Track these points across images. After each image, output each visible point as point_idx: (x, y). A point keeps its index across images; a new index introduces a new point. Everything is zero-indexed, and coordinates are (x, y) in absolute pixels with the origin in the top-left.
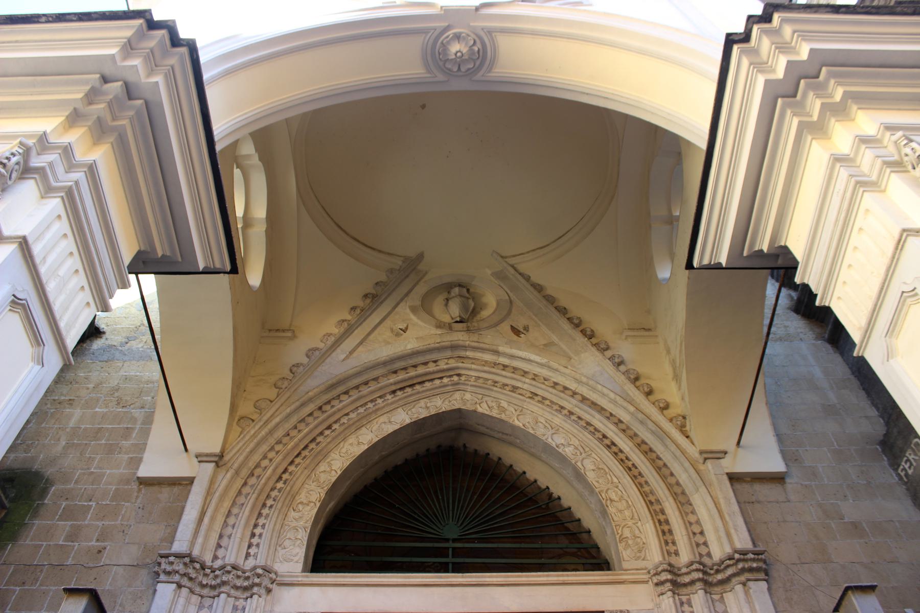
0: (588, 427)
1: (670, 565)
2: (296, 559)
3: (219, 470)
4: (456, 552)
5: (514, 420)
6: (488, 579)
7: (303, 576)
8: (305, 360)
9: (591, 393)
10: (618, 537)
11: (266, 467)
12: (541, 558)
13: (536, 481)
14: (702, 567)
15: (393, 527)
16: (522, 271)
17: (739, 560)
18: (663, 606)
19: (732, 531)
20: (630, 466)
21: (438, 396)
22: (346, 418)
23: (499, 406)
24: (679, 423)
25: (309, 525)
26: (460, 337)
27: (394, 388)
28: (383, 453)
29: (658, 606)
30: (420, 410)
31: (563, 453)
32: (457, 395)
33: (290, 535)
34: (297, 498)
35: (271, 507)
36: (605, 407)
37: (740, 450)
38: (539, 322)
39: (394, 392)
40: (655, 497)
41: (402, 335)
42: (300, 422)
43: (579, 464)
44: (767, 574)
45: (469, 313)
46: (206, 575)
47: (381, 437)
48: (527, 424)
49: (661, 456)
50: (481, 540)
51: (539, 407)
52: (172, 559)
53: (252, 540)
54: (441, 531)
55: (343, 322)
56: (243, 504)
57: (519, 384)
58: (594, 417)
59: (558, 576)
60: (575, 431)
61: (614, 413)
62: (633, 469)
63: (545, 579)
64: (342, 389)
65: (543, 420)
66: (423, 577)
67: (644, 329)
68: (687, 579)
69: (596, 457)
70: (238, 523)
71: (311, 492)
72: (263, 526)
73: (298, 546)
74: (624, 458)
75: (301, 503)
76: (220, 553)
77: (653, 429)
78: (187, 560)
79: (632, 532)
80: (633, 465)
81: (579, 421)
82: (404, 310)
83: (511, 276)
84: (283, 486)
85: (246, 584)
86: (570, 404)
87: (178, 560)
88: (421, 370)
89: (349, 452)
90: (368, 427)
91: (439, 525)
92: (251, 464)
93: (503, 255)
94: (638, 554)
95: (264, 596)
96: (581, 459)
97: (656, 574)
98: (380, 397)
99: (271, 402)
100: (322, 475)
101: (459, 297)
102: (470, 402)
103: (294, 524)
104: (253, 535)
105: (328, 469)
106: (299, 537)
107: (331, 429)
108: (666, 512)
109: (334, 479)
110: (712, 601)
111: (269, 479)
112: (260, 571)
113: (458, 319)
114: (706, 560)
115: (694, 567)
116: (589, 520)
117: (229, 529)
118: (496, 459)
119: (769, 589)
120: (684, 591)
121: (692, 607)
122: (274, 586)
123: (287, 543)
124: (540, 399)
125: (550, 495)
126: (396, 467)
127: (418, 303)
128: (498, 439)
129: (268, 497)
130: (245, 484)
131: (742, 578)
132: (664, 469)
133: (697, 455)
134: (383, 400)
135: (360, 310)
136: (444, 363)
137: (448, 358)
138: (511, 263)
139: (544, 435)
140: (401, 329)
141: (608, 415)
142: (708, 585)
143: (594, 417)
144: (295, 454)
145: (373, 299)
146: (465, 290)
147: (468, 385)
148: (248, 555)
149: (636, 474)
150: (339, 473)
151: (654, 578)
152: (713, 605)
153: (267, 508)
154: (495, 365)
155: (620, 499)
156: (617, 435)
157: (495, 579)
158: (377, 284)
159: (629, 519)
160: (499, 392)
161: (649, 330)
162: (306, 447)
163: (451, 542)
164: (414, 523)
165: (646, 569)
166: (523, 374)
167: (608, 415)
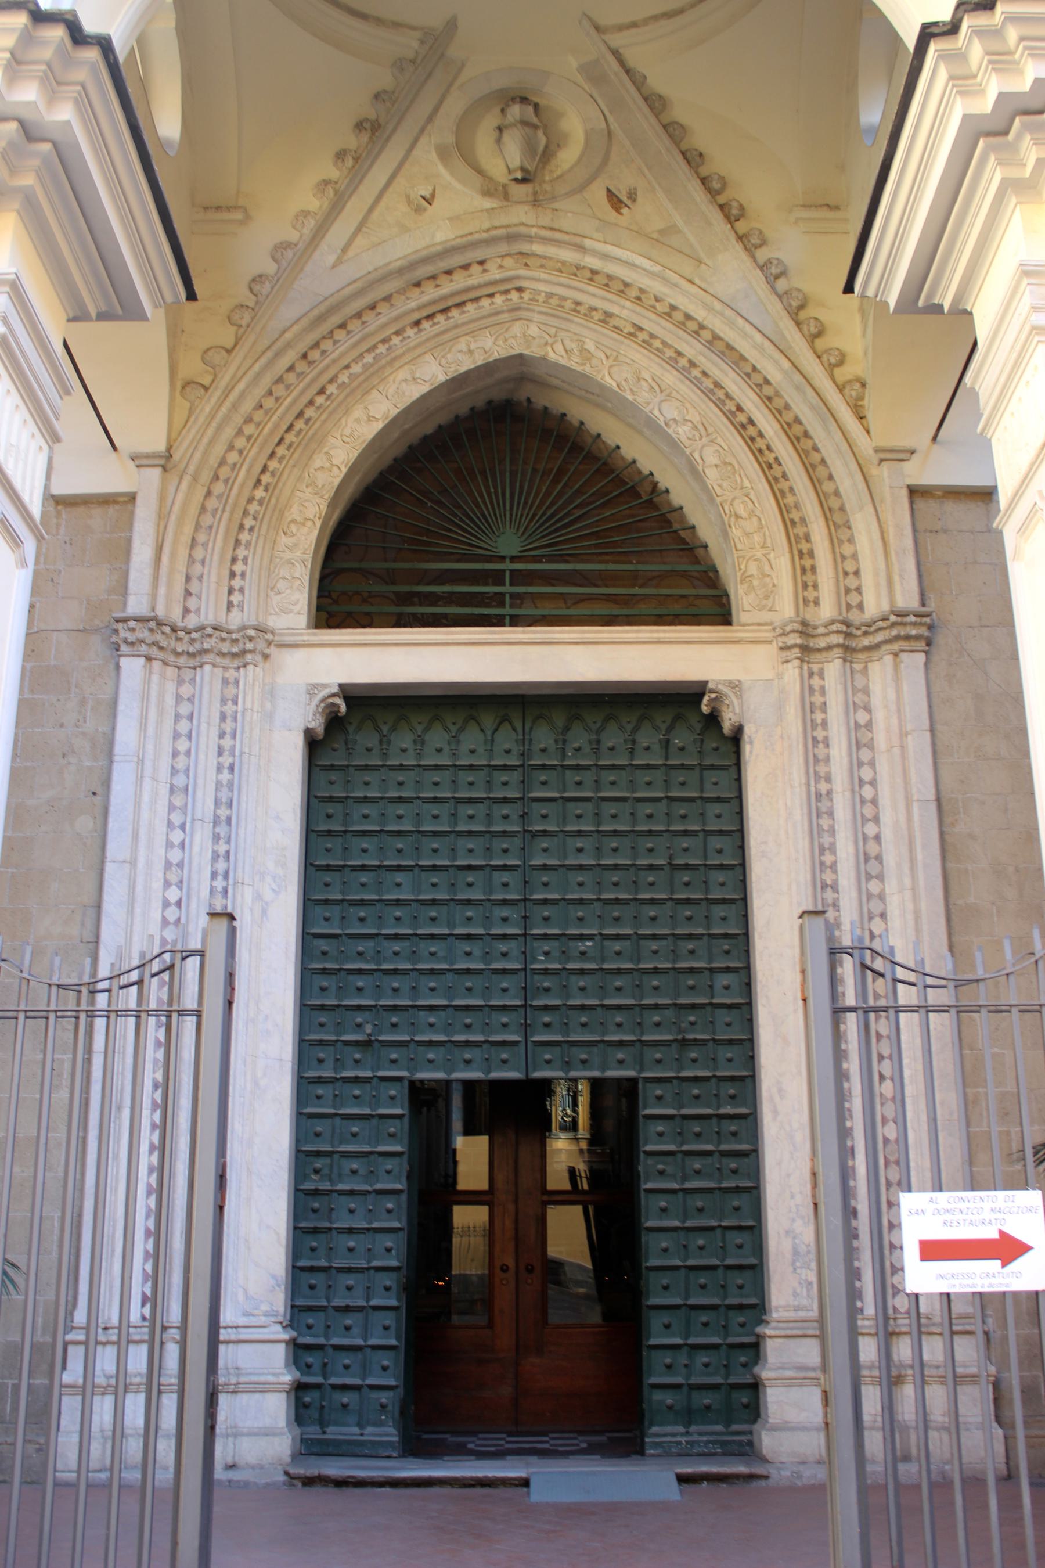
0: (716, 390)
1: (804, 623)
2: (296, 609)
4: (518, 578)
7: (309, 634)
8: (271, 268)
10: (739, 574)
11: (235, 465)
12: (634, 586)
13: (634, 462)
14: (844, 628)
15: (425, 538)
16: (631, 63)
17: (894, 625)
18: (786, 678)
19: (896, 578)
20: (772, 461)
21: (487, 331)
22: (346, 372)
23: (583, 350)
24: (854, 393)
25: (309, 557)
26: (520, 215)
27: (416, 316)
28: (406, 426)
29: (780, 676)
30: (460, 356)
31: (674, 436)
32: (517, 328)
33: (284, 572)
34: (286, 514)
35: (252, 529)
37: (935, 447)
39: (417, 323)
40: (800, 514)
41: (425, 210)
43: (696, 455)
44: (928, 644)
45: (537, 158)
47: (402, 406)
48: (623, 383)
49: (819, 446)
50: (551, 559)
52: (132, 624)
53: (233, 583)
55: (326, 185)
56: (211, 527)
57: (614, 309)
58: (727, 375)
59: (651, 631)
61: (758, 367)
62: (775, 466)
64: (335, 320)
65: (648, 377)
66: (470, 633)
67: (828, 205)
68: (822, 643)
69: (723, 444)
72: (245, 560)
74: (764, 448)
75: (294, 521)
76: (192, 603)
78: (153, 624)
79: (760, 568)
80: (776, 459)
81: (704, 379)
82: (426, 153)
84: (264, 494)
85: (235, 650)
86: (691, 348)
87: (140, 625)
88: (460, 281)
89: (356, 433)
91: (487, 541)
92: (213, 461)
93: (602, 22)
94: (764, 602)
95: (261, 665)
97: (783, 634)
98: (397, 333)
99: (229, 352)
101: (519, 126)
103: (288, 555)
104: (233, 575)
105: (327, 465)
106: (297, 575)
108: (813, 539)
109: (337, 482)
110: (852, 672)
111: (242, 486)
112: (251, 632)
114: (855, 617)
115: (834, 627)
116: (706, 532)
117: (197, 569)
119: (926, 664)
120: (818, 656)
121: (823, 679)
122: (272, 651)
123: (281, 585)
124: (647, 338)
125: (655, 485)
126: (425, 439)
127: (451, 139)
129: (245, 513)
130: (209, 493)
131: (896, 647)
132: (820, 469)
133: (871, 452)
134: (400, 338)
137: (503, 256)
138: (614, 44)
139: (648, 404)
140: (424, 198)
141: (749, 370)
142: (848, 651)
143: (727, 375)
144: (276, 440)
145: (373, 134)
146: (531, 109)
147: (533, 311)
148: (230, 605)
149: (779, 475)
150: (344, 470)
151: (780, 639)
152: (852, 678)
154: (578, 269)
155: (749, 515)
157: (566, 636)
158: (377, 96)
161: (837, 208)
162: (290, 428)
163: (508, 560)
165: (771, 624)
166: (622, 287)
167: (749, 370)
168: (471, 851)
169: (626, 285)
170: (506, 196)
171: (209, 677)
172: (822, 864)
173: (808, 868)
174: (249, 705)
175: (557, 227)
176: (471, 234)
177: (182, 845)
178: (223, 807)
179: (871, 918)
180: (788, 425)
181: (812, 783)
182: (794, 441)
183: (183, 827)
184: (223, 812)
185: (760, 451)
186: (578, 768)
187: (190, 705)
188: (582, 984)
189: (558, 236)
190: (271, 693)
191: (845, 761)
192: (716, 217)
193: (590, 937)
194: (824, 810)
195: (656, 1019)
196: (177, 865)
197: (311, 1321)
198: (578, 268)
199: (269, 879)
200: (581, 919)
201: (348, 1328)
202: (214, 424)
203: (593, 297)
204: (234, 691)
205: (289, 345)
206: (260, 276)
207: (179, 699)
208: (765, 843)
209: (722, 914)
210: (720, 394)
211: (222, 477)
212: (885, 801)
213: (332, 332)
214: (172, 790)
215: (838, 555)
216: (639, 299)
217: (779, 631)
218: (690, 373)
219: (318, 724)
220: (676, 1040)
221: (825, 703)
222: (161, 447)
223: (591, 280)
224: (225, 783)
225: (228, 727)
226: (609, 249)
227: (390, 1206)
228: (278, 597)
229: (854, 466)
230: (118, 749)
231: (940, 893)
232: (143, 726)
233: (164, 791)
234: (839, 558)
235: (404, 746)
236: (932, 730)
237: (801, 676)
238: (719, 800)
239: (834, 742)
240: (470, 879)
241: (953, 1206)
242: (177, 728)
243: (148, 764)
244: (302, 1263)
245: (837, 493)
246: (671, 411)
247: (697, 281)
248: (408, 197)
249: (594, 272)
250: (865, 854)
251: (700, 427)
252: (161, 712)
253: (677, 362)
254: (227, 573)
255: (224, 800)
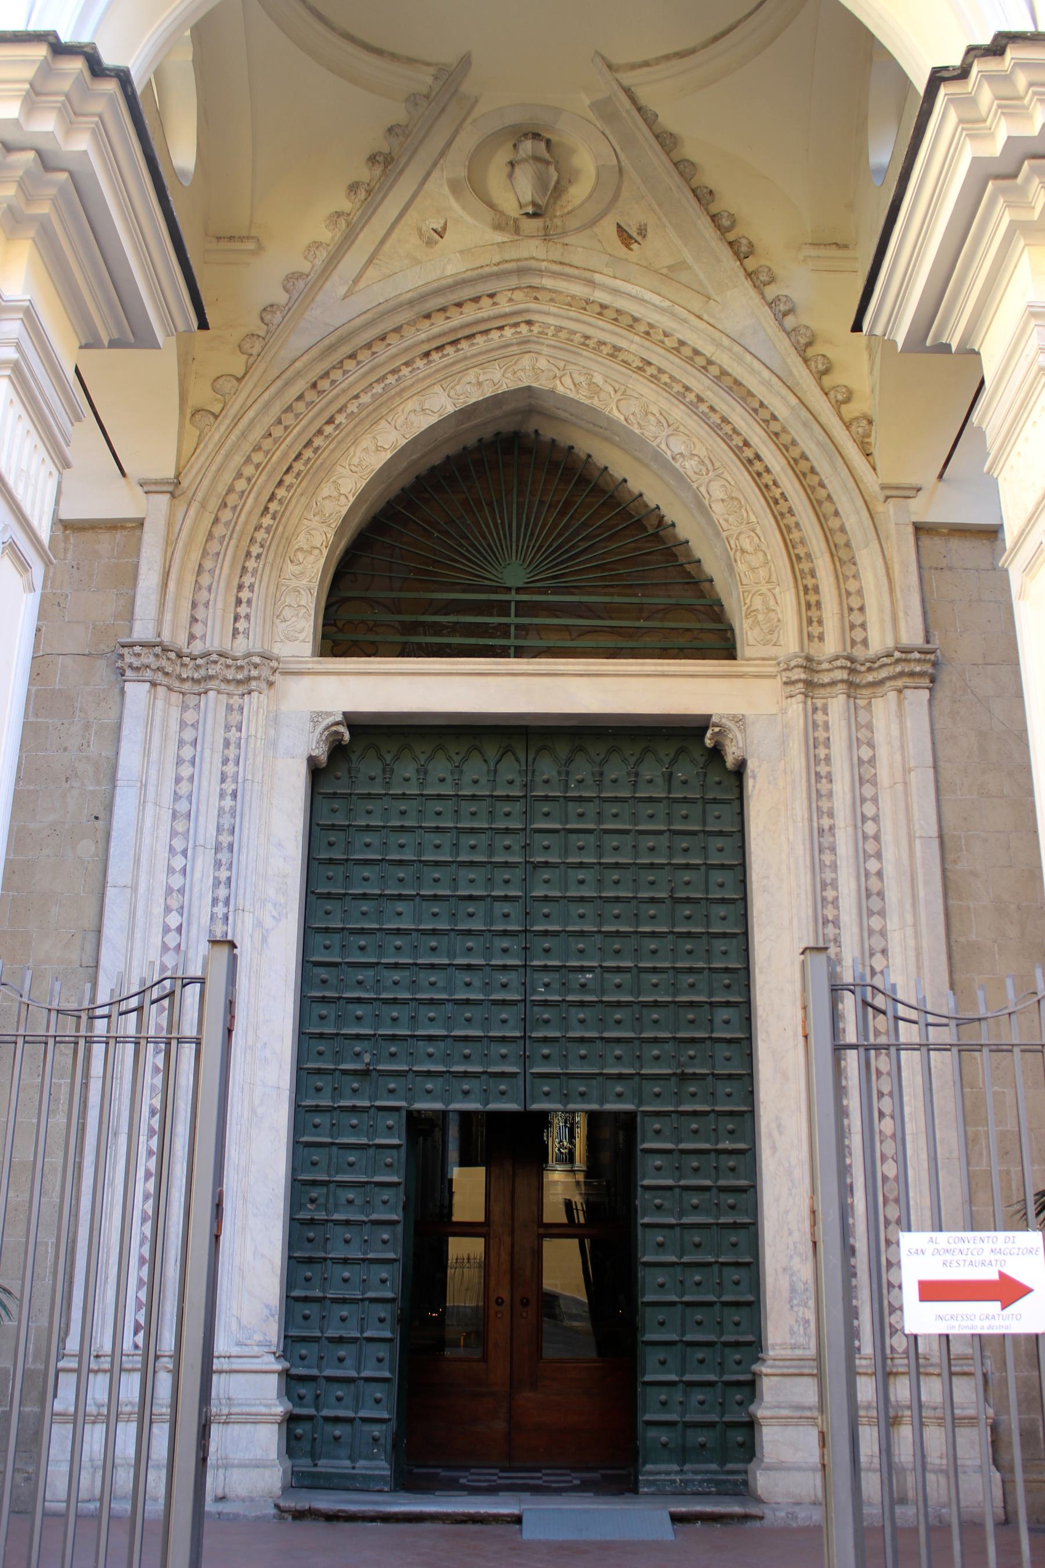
0: (723, 425)
1: (809, 659)
2: (302, 636)
3: (176, 501)
4: (524, 608)
5: (612, 409)
6: (562, 667)
7: (313, 662)
8: (282, 298)
9: (735, 364)
10: (744, 608)
11: (243, 492)
12: (639, 619)
13: (641, 495)
14: (849, 664)
15: (431, 568)
16: (643, 101)
17: (898, 661)
19: (901, 615)
20: (778, 496)
21: (496, 363)
22: (356, 403)
23: (591, 384)
24: (860, 430)
25: (315, 585)
26: (531, 249)
27: (426, 347)
28: (414, 457)
29: (784, 711)
30: (468, 388)
31: (681, 470)
32: (526, 361)
34: (293, 542)
35: (258, 556)
36: (754, 391)
37: (941, 484)
38: (664, 219)
39: (427, 354)
40: (805, 550)
41: (437, 243)
42: (286, 411)
43: (703, 489)
44: (932, 681)
45: (548, 194)
46: (183, 665)
47: (410, 437)
48: (631, 417)
49: (826, 482)
50: (556, 591)
51: (652, 390)
52: (137, 649)
53: (239, 610)
54: (500, 576)
55: (338, 217)
56: (218, 554)
57: (622, 344)
58: (734, 410)
60: (703, 434)
61: (766, 403)
62: (781, 501)
63: (638, 668)
64: (346, 349)
65: (656, 411)
66: (474, 664)
67: (837, 244)
68: (826, 678)
69: (729, 479)
70: (215, 584)
71: (313, 532)
72: (251, 587)
73: (303, 617)
74: (771, 483)
75: (301, 549)
76: (198, 629)
77: (821, 438)
78: (158, 650)
79: (765, 602)
80: (782, 494)
81: (711, 414)
82: (438, 187)
83: (624, 114)
84: (271, 522)
85: (240, 677)
86: (699, 383)
87: (145, 650)
88: (470, 313)
89: (363, 463)
90: (389, 420)
91: (494, 572)
92: (221, 488)
93: (615, 60)
94: (769, 637)
95: (265, 692)
96: (707, 480)
98: (407, 364)
99: (239, 380)
100: (327, 502)
101: (531, 161)
102: (546, 373)
103: (294, 583)
104: (239, 602)
105: (335, 494)
106: (303, 603)
107: (333, 422)
108: (818, 574)
109: (344, 511)
110: (855, 708)
111: (250, 513)
112: (257, 660)
113: (530, 210)
114: (859, 652)
115: (838, 663)
116: (712, 566)
117: (204, 595)
118: (584, 457)
119: (930, 701)
120: (822, 692)
121: (827, 714)
122: (277, 678)
123: (287, 613)
124: (655, 372)
126: (433, 468)
127: (463, 173)
128: (587, 431)
129: (252, 540)
130: (216, 520)
131: (899, 683)
133: (877, 489)
134: (410, 369)
135: (366, 191)
136: (506, 299)
137: (513, 289)
138: (626, 82)
139: (656, 438)
140: (435, 231)
141: (757, 405)
143: (734, 410)
144: (285, 469)
145: (386, 167)
146: (543, 145)
147: (542, 344)
148: (235, 632)
149: (785, 510)
150: (352, 499)
151: (784, 674)
152: (856, 713)
153: (253, 559)
154: (587, 304)
156: (764, 442)
157: (570, 667)
158: (390, 130)
159: (764, 582)
160: (591, 359)
161: (846, 247)
162: (299, 456)
163: (513, 592)
164: (464, 564)
165: (775, 659)
166: (631, 323)
167: (757, 405)
168: (472, 881)
169: (636, 320)
170: (517, 230)
171: (214, 703)
172: (824, 899)
173: (810, 903)
174: (252, 732)
175: (567, 261)
176: (482, 267)
177: (184, 871)
178: (225, 833)
179: (872, 955)
180: (795, 460)
181: (815, 818)
182: (801, 477)
183: (184, 853)
184: (225, 839)
185: (767, 486)
186: (581, 799)
187: (194, 732)
188: (581, 1016)
189: (568, 270)
190: (275, 720)
191: (848, 797)
192: (725, 253)
193: (591, 970)
194: (826, 845)
195: (656, 1052)
196: (178, 891)
197: (304, 1352)
198: (588, 302)
199: (269, 906)
200: (581, 951)
201: (341, 1360)
202: (223, 452)
203: (602, 331)
204: (239, 718)
205: (299, 374)
206: (272, 306)
207: (183, 724)
208: (767, 877)
209: (723, 948)
210: (728, 429)
211: (230, 505)
212: (887, 837)
213: (342, 362)
214: (174, 816)
215: (843, 591)
216: (647, 333)
217: (783, 666)
218: (697, 408)
219: (321, 752)
220: (674, 1074)
221: (828, 739)
222: (170, 473)
223: (600, 314)
224: (227, 809)
225: (232, 753)
226: (619, 284)
227: (386, 1237)
228: (284, 624)
229: (860, 503)
230: (120, 774)
231: (941, 930)
232: (147, 752)
233: (167, 816)
234: (844, 594)
235: (407, 775)
236: (935, 767)
237: (805, 710)
238: (721, 833)
239: (837, 777)
240: (471, 910)
241: (952, 1246)
242: (181, 753)
243: (151, 789)
244: (296, 1293)
245: (842, 529)
246: (678, 445)
247: (705, 317)
248: (419, 230)
249: (603, 307)
250: (867, 890)
251: (707, 462)
252: (165, 738)
253: (685, 397)
254: (233, 600)
255: (226, 827)
